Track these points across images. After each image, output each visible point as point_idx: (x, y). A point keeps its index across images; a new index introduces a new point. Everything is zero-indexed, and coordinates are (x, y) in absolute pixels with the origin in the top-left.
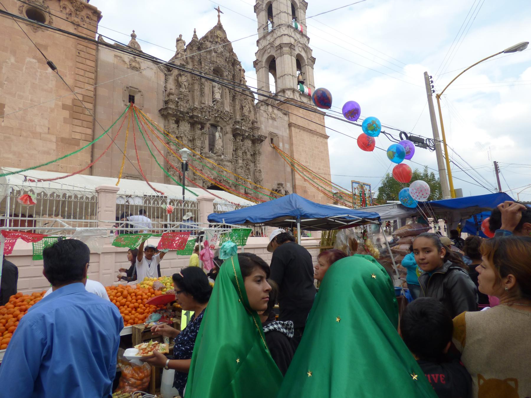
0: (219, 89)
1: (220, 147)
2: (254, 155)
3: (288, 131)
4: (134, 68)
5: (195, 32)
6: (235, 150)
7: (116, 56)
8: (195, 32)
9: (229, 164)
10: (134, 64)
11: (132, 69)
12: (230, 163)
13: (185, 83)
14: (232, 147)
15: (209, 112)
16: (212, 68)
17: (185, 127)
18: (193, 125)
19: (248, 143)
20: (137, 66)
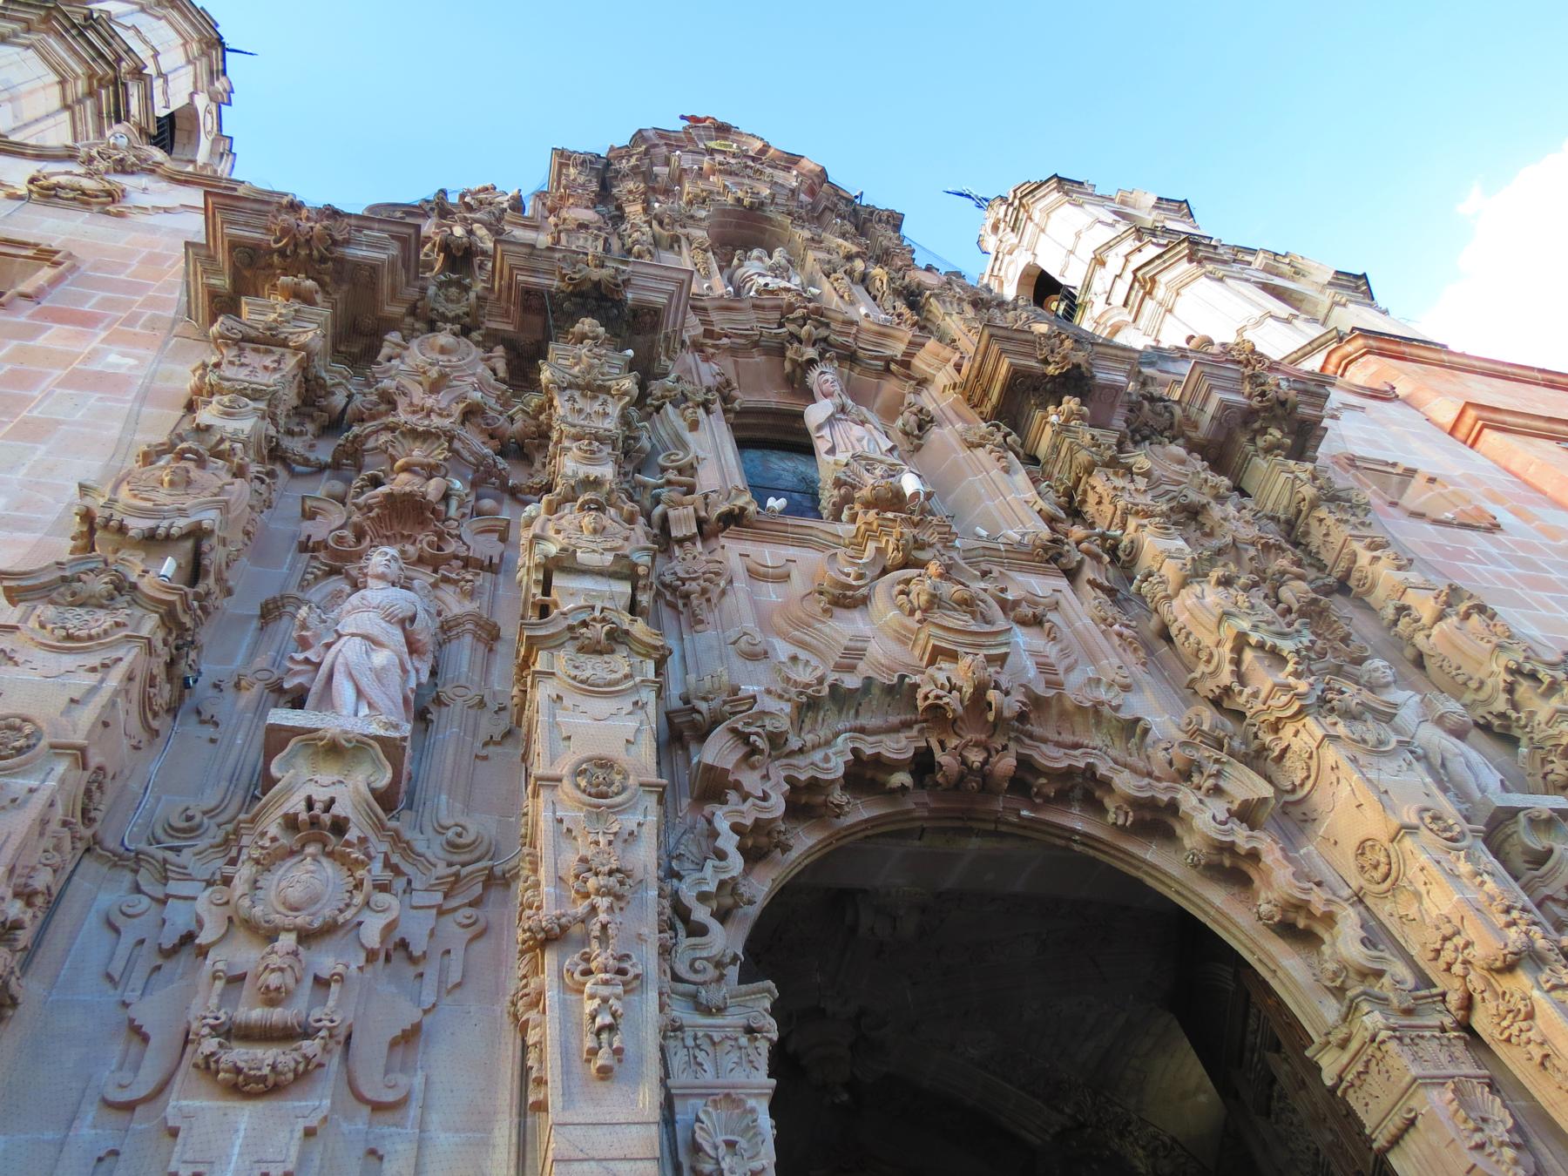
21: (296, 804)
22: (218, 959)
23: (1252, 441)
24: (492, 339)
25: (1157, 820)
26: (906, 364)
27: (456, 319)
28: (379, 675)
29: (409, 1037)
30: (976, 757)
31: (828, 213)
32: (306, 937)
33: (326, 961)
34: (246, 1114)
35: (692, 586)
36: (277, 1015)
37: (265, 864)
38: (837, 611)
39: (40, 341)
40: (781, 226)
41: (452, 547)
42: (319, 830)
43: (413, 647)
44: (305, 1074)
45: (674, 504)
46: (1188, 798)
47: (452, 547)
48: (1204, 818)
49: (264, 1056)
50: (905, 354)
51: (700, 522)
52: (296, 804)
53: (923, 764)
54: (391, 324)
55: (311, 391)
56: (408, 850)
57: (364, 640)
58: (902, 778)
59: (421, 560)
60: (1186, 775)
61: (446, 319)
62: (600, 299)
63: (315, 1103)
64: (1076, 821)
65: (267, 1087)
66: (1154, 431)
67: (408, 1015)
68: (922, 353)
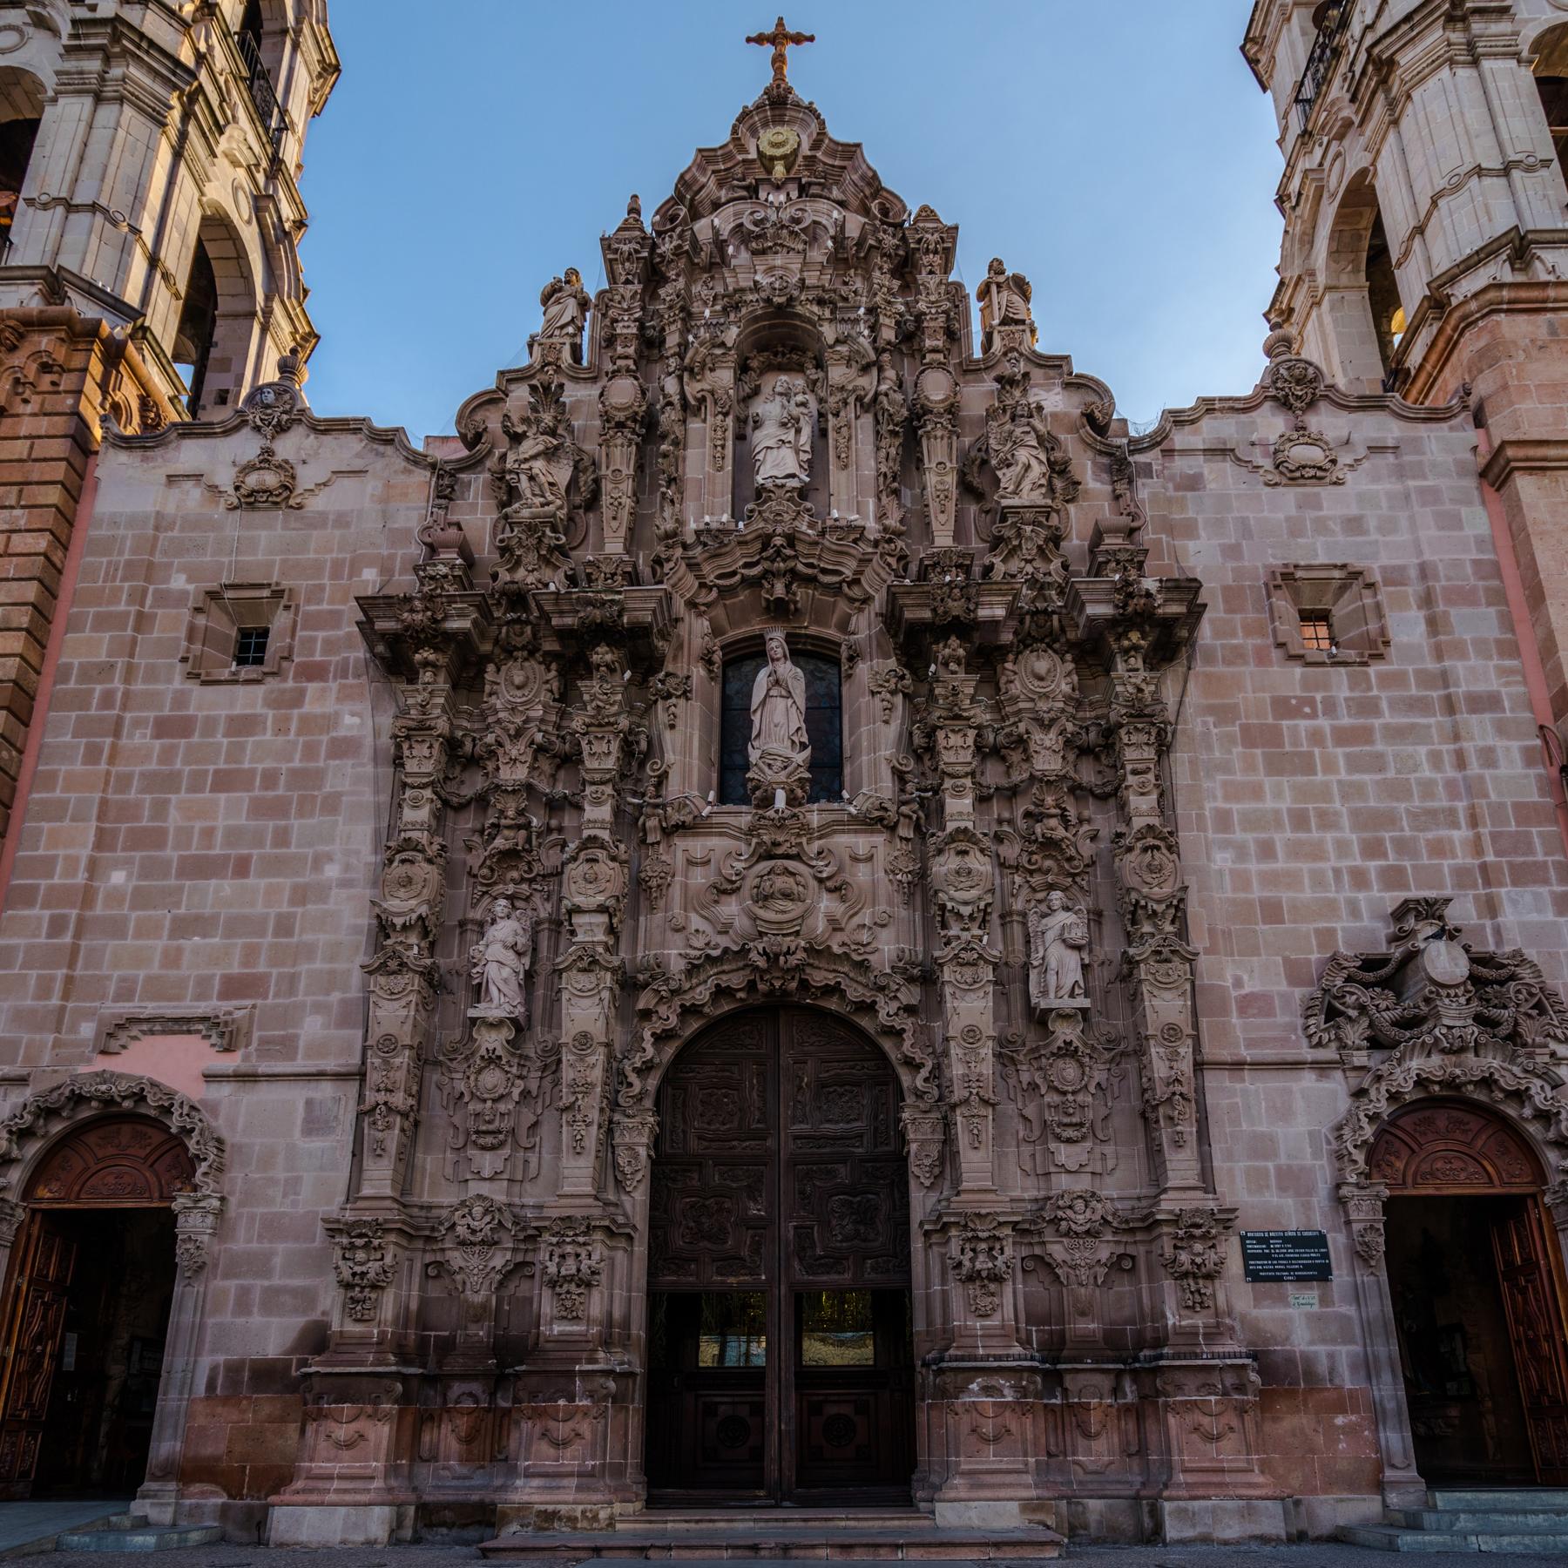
0: (790, 423)
1: (783, 748)
2: (1099, 746)
3: (1477, 520)
4: (251, 501)
5: (634, 210)
6: (922, 749)
7: (172, 479)
8: (634, 210)
9: (862, 843)
10: (252, 480)
11: (251, 506)
12: (879, 839)
13: (539, 466)
14: (891, 732)
15: (692, 566)
16: (732, 334)
17: (519, 692)
18: (572, 662)
19: (1043, 678)
20: (271, 479)
21: (483, 1052)
22: (471, 1107)
23: (1118, 639)
24: (548, 659)
25: (869, 1008)
26: (856, 582)
27: (524, 648)
28: (505, 981)
29: (535, 1125)
30: (777, 984)
31: (874, 253)
32: (494, 1101)
33: (502, 1107)
34: (488, 1155)
35: (653, 883)
36: (491, 1127)
37: (479, 1072)
38: (724, 898)
39: (307, 708)
40: (810, 321)
41: (537, 868)
42: (492, 1060)
43: (519, 954)
44: (502, 1144)
45: (649, 816)
46: (881, 999)
47: (537, 868)
48: (886, 1010)
49: (489, 1140)
50: (856, 573)
51: (663, 829)
52: (483, 1052)
53: (751, 986)
54: (488, 658)
55: (451, 745)
56: (527, 1058)
57: (498, 953)
58: (741, 995)
59: (523, 880)
60: (882, 989)
61: (517, 649)
62: (606, 632)
63: (506, 1151)
64: (833, 1004)
65: (493, 1148)
66: (1036, 640)
67: (533, 1119)
68: (868, 571)
